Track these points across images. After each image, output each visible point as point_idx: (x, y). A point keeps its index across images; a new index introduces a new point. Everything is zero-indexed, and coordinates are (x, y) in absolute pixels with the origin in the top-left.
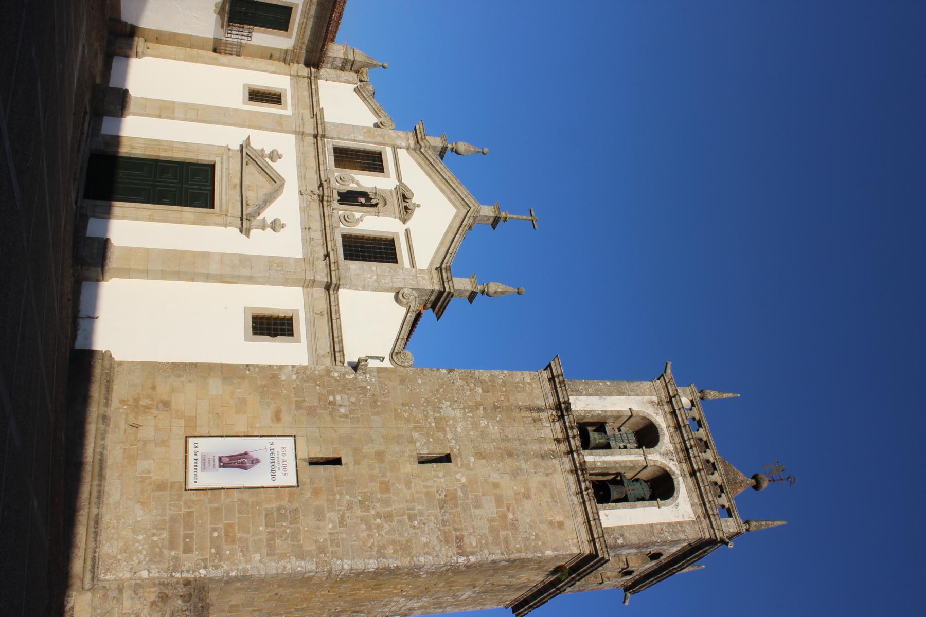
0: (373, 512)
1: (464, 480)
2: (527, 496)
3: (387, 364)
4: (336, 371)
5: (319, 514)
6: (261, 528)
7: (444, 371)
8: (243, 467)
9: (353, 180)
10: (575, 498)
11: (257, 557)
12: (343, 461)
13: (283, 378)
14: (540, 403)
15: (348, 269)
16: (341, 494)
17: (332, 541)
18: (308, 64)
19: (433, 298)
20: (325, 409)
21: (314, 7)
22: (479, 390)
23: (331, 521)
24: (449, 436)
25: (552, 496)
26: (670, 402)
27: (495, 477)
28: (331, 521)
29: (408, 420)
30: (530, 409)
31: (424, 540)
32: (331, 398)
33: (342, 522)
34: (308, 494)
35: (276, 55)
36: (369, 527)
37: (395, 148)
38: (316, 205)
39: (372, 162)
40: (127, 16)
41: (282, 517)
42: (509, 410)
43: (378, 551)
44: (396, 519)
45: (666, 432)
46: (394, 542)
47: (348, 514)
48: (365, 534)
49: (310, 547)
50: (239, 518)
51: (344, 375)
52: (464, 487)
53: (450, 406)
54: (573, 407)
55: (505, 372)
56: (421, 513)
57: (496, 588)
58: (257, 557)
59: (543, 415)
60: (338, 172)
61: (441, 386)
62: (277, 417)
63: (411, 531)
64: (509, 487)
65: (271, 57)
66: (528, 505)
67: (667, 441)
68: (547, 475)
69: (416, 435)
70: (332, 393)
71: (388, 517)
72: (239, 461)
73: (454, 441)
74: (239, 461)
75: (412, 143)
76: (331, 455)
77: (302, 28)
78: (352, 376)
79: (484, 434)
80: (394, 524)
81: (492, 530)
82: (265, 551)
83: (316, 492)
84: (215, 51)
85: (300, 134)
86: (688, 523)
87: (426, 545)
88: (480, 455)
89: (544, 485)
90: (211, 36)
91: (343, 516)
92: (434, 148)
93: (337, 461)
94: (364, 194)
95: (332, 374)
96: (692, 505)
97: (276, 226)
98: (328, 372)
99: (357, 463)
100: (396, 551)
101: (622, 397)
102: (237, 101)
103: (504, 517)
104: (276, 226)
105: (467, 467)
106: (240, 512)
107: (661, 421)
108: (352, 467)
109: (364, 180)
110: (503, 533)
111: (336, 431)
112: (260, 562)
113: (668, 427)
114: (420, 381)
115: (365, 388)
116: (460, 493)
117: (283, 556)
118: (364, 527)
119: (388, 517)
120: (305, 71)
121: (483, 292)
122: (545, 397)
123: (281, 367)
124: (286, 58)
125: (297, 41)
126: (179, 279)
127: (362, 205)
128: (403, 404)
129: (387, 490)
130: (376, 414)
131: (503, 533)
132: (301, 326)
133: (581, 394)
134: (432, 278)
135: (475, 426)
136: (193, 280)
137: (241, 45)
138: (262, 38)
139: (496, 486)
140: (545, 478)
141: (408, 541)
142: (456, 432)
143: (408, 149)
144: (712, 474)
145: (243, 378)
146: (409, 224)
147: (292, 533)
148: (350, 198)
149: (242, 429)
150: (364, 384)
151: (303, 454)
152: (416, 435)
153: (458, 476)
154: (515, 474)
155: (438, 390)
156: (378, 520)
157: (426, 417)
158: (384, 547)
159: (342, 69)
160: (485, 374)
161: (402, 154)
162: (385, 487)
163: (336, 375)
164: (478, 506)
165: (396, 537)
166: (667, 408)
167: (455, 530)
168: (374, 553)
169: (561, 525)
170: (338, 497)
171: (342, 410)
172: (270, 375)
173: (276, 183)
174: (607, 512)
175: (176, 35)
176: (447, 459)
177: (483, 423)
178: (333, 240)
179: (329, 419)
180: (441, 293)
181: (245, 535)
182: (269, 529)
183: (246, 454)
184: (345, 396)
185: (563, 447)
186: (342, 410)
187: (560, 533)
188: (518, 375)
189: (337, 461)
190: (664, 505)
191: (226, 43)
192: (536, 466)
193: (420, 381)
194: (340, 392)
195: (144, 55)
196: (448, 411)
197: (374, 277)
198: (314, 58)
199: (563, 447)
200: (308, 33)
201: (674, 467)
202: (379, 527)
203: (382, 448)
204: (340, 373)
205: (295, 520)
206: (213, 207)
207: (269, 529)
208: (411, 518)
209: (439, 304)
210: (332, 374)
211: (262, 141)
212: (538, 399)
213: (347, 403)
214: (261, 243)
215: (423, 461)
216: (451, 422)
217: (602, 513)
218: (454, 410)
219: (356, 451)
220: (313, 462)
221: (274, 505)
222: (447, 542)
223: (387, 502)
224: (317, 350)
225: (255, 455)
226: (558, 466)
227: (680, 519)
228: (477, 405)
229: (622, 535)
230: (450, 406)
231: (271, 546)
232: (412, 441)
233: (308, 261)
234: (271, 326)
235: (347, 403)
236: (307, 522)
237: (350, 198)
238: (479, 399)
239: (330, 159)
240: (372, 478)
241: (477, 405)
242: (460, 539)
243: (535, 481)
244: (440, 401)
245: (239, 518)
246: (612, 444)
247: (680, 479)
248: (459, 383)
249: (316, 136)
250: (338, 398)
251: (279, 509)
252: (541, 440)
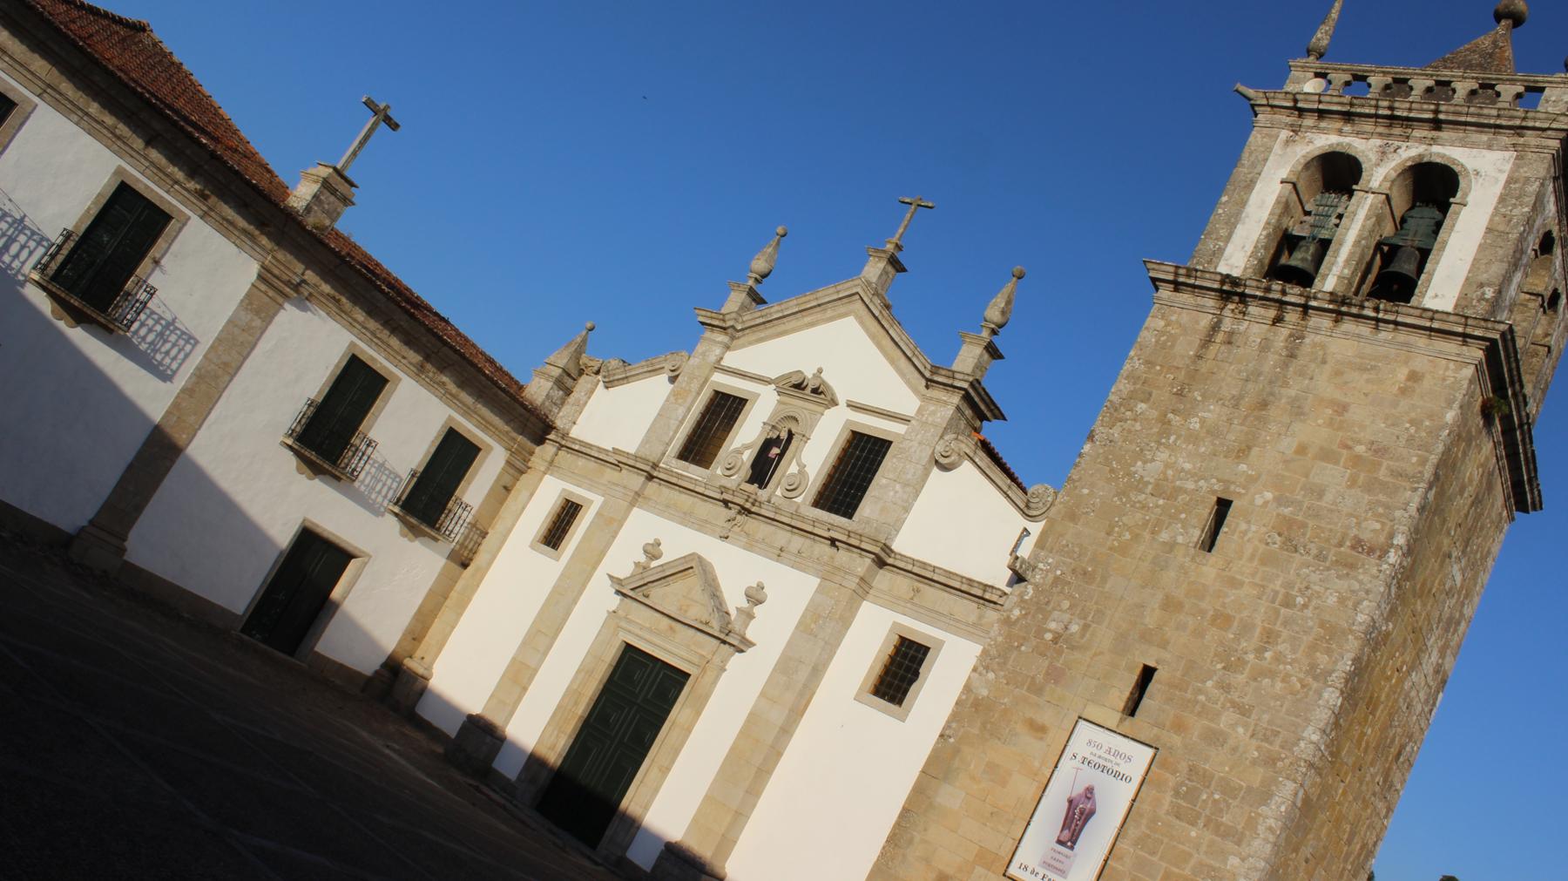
0: (1251, 657)
1: (1269, 495)
2: (1342, 408)
3: (1036, 528)
5: (1215, 738)
6: (1193, 834)
7: (1087, 448)
8: (1088, 815)
9: (739, 452)
10: (1383, 335)
11: (1234, 861)
12: (1152, 664)
13: (985, 692)
14: (1205, 321)
15: (868, 522)
16: (1200, 691)
17: (1266, 739)
18: (540, 441)
19: (968, 412)
20: (1060, 652)
21: (464, 396)
22: (1141, 407)
23: (1233, 726)
24: (1190, 485)
25: (1363, 369)
26: (1301, 112)
27: (1288, 445)
28: (1233, 726)
29: (1136, 537)
30: (1208, 341)
31: (1332, 600)
32: (1049, 636)
33: (1244, 711)
34: (1176, 740)
35: (507, 480)
36: (1272, 674)
37: (718, 367)
38: (751, 524)
39: (724, 410)
40: (368, 665)
41: (1191, 796)
42: (1193, 375)
43: (1316, 678)
44: (1278, 627)
45: (1347, 140)
46: (1313, 648)
47: (1235, 696)
48: (1279, 685)
49: (1257, 776)
50: (1161, 858)
51: (1023, 601)
52: (1279, 501)
53: (1145, 462)
54: (1236, 273)
55: (1132, 353)
56: (1289, 585)
57: (1470, 521)
58: (1234, 861)
59: (1227, 325)
60: (718, 468)
61: (1107, 462)
62: (1039, 729)
63: (1308, 613)
64: (1313, 430)
65: (507, 489)
66: (1357, 413)
67: (1361, 145)
68: (1324, 362)
69: (1164, 536)
70: (1040, 632)
71: (1269, 637)
72: (1077, 818)
73: (1202, 483)
74: (1077, 818)
75: (721, 338)
76: (1134, 677)
77: (486, 426)
78: (1030, 589)
79: (1213, 432)
80: (1285, 633)
81: (1368, 488)
82: (1230, 845)
83: (1179, 727)
84: (465, 566)
85: (637, 498)
86: (1516, 167)
87: (1342, 601)
88: (1242, 452)
89: (1338, 373)
90: (443, 561)
91: (1234, 705)
92: (743, 308)
93: (1147, 674)
94: (768, 444)
95: (1013, 618)
96: (1490, 147)
97: (755, 597)
98: (1007, 622)
99: (1164, 645)
100: (1328, 652)
101: (1258, 186)
102: (551, 567)
103: (1357, 460)
104: (755, 597)
105: (1252, 480)
106: (1153, 854)
107: (1326, 139)
108: (1167, 656)
109: (746, 435)
110: (1382, 474)
111: (1101, 653)
112: (1243, 860)
113: (1340, 132)
114: (1086, 491)
115: (1057, 579)
116: (1287, 511)
117: (1251, 824)
118: (1267, 681)
119: (1269, 637)
120: (548, 449)
121: (994, 332)
122: (1200, 309)
123: (968, 688)
124: (518, 468)
125: (500, 440)
126: (770, 772)
127: (781, 456)
128: (1108, 534)
129: (1228, 619)
130: (1104, 580)
131: (1382, 474)
132: (920, 630)
133: (1221, 251)
134: (938, 401)
135: (1193, 438)
136: (780, 755)
137: (473, 525)
138: (475, 490)
139: (1302, 450)
140: (1328, 368)
141: (1322, 625)
142: (1188, 472)
143: (728, 348)
144: (1454, 91)
145: (956, 751)
146: (841, 399)
147: (1223, 793)
148: (763, 468)
149: (1031, 790)
150: (1051, 576)
151: (1113, 718)
152: (1164, 536)
153: (1259, 501)
154: (1298, 410)
155: (1112, 471)
156: (1268, 655)
157: (1144, 507)
158: (1313, 666)
159: (568, 392)
160: (1122, 386)
161: (732, 359)
162: (1222, 619)
163: (1017, 612)
164: (1321, 494)
165: (1307, 639)
166: (1309, 121)
167: (1340, 545)
168: (1315, 685)
169: (1414, 377)
170: (1202, 698)
171: (1074, 628)
172: (972, 709)
173: (691, 567)
174: (1430, 293)
175: (420, 612)
176: (1223, 506)
177: (1195, 424)
178: (814, 522)
179: (1077, 655)
180: (967, 398)
181: (1192, 862)
182: (1201, 823)
183: (1070, 802)
184: (1056, 614)
185: (1292, 316)
186: (1074, 628)
187: (1427, 383)
188: (1146, 336)
189: (1147, 674)
190: (1466, 195)
191: (462, 545)
192: (1301, 373)
193: (1086, 491)
194: (1045, 619)
195: (429, 668)
196: (1149, 470)
197: (898, 487)
198: (535, 427)
199: (1292, 316)
200: (497, 421)
201: (1411, 151)
202: (1279, 658)
203: (1160, 596)
204: (1017, 605)
205: (1206, 779)
206: (687, 676)
207: (1201, 823)
208: (1288, 603)
209: (983, 407)
210: (1013, 618)
211: (622, 558)
212: (1197, 323)
213: (1066, 617)
214: (770, 632)
215: (1210, 543)
216: (1170, 472)
217: (1429, 302)
218: (1153, 460)
219: (1146, 637)
220: (1132, 708)
221: (1168, 798)
222: (1352, 566)
223: (1246, 628)
224: (968, 624)
225: (1079, 789)
226: (1318, 338)
227: (1503, 178)
228: (1164, 422)
229: (1481, 285)
230: (1145, 462)
231: (1227, 833)
232: (1171, 546)
233: (828, 575)
234: (899, 674)
235: (1066, 617)
236: (1217, 763)
237: (763, 468)
238: (1154, 414)
239: (692, 472)
240: (1199, 633)
241: (1164, 422)
242: (1358, 544)
243: (1324, 386)
244: (1129, 474)
245: (1161, 858)
246: (1324, 234)
247: (1436, 149)
248: (1116, 432)
249: (650, 477)
250: (1053, 625)
251: (1177, 794)
252: (1265, 346)
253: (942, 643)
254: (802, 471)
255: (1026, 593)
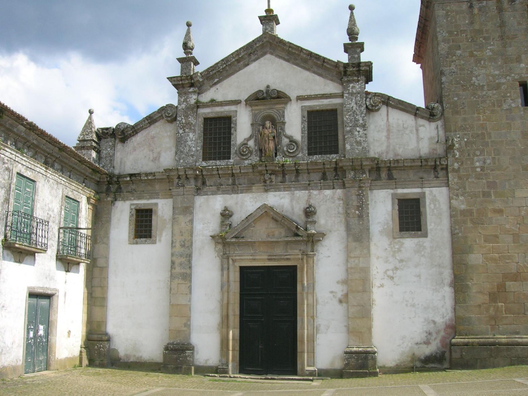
4: (453, 165)
9: (244, 144)
22: (459, 52)
32: (478, 170)
69: (505, 107)
70: (474, 168)
73: (508, 78)
115: (466, 142)
132: (410, 192)
142: (499, 75)
146: (293, 95)
150: (463, 143)
152: (505, 107)
155: (462, 86)
161: (205, 98)
194: (472, 163)
234: (410, 218)
244: (473, 85)
248: (453, 67)
253: (156, 204)
254: (292, 141)
255: (456, 155)
